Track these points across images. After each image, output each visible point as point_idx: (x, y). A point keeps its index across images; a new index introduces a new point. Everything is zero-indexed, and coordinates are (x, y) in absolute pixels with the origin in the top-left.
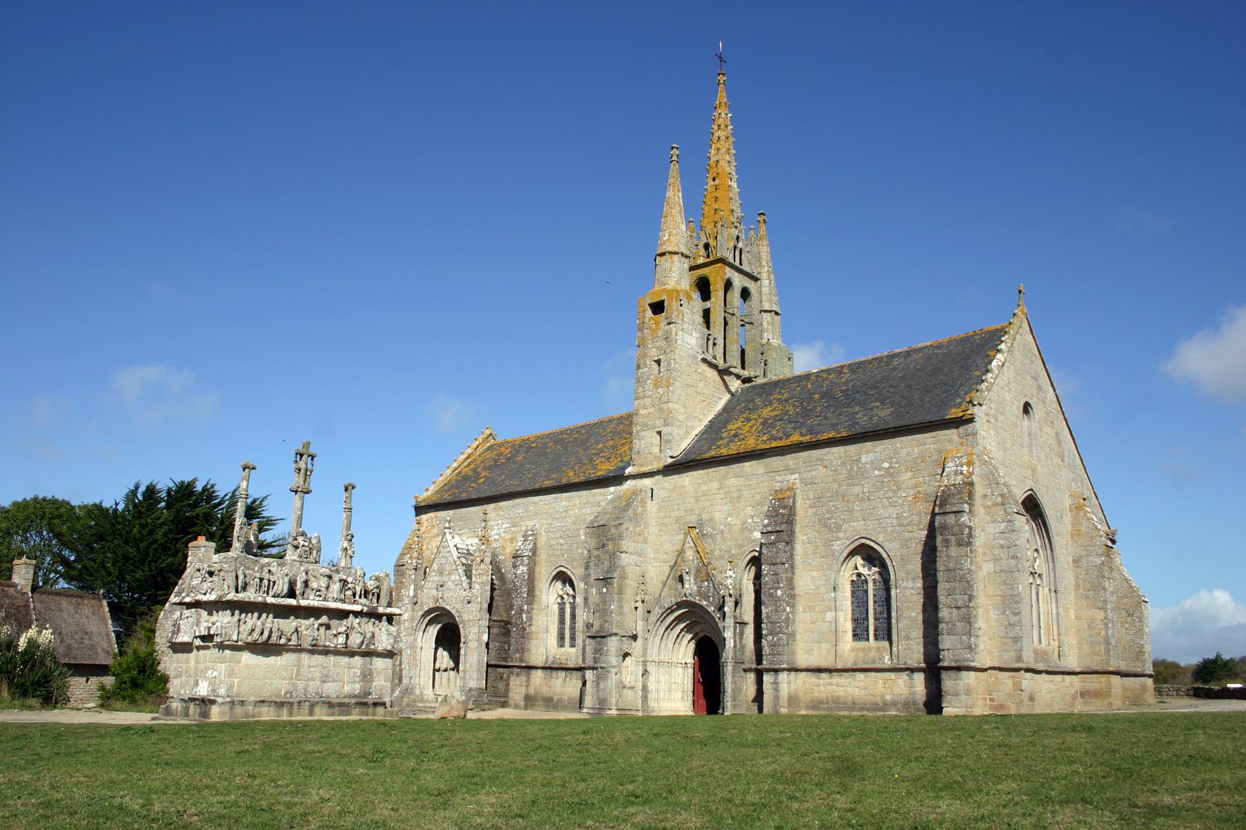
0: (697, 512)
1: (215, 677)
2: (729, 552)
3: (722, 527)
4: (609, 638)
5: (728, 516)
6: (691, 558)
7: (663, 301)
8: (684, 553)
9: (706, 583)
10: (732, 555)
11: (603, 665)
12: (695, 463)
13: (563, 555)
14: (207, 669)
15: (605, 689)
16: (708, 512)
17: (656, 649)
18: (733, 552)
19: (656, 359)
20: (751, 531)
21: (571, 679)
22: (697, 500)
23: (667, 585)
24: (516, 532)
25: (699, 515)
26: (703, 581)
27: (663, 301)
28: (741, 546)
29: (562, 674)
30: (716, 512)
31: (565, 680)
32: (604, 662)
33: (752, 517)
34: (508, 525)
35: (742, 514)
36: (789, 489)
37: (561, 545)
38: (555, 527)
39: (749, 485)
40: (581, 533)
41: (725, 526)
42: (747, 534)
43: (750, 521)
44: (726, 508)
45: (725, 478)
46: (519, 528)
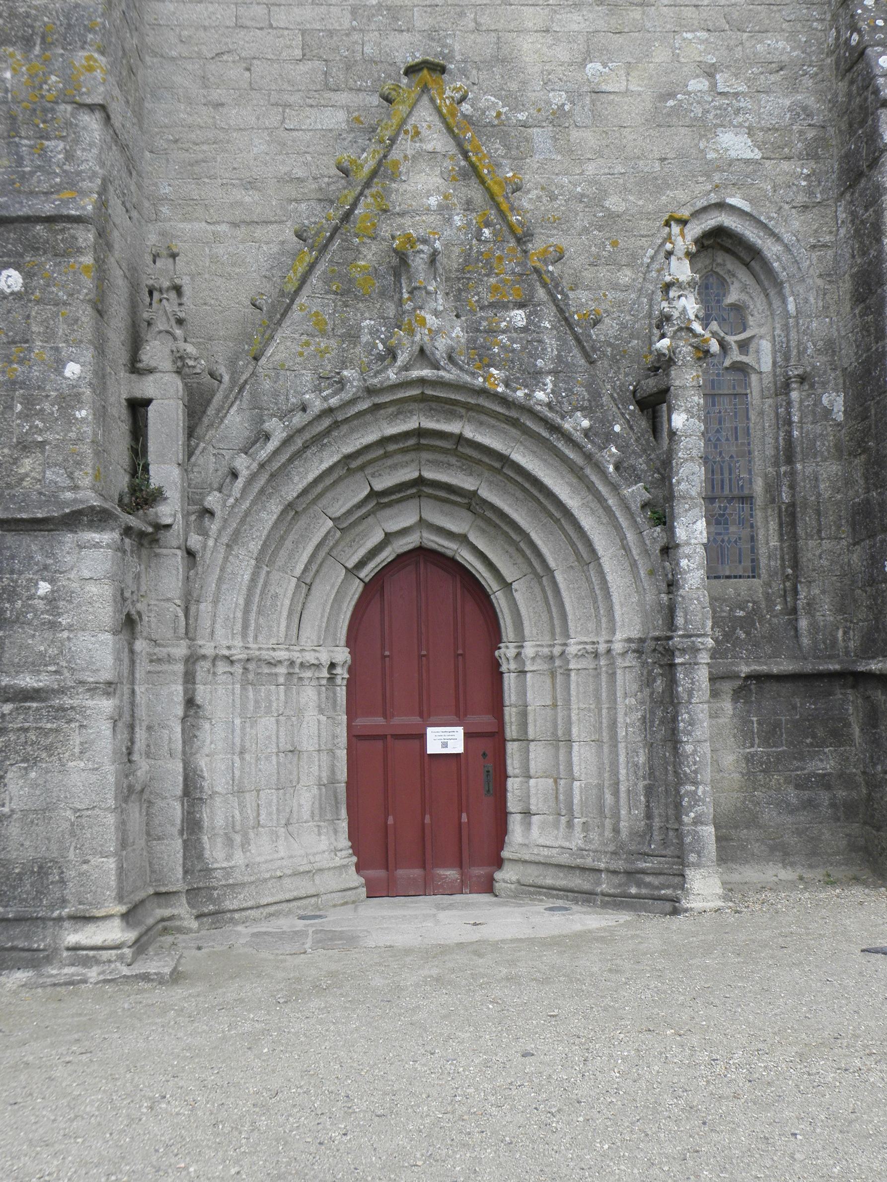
0: (421, 21)
2: (597, 201)
4: (69, 538)
5: (587, 57)
6: (433, 201)
8: (394, 177)
9: (519, 317)
10: (613, 216)
11: (27, 681)
15: (46, 811)
16: (477, 29)
17: (233, 600)
18: (614, 203)
23: (296, 314)
25: (432, 34)
26: (500, 306)
28: (657, 185)
32: (35, 666)
33: (710, 72)
35: (661, 55)
41: (574, 96)
42: (682, 137)
43: (698, 84)
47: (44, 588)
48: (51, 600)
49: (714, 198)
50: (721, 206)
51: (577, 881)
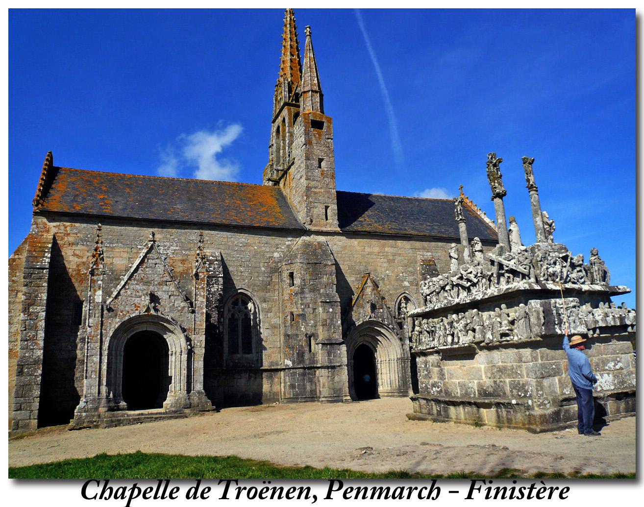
1: (621, 368)
3: (383, 276)
5: (386, 270)
7: (324, 122)
12: (366, 233)
13: (244, 280)
14: (605, 362)
19: (321, 157)
20: (403, 281)
21: (256, 378)
22: (363, 256)
24: (187, 255)
27: (324, 122)
28: (396, 289)
29: (245, 376)
30: (378, 266)
31: (250, 378)
34: (177, 248)
36: (430, 261)
37: (242, 272)
38: (234, 257)
39: (400, 254)
40: (262, 265)
43: (401, 275)
44: (385, 265)
45: (384, 246)
46: (193, 253)
47: (339, 352)
48: (340, 353)
49: (404, 292)
50: (405, 293)
51: (390, 394)
